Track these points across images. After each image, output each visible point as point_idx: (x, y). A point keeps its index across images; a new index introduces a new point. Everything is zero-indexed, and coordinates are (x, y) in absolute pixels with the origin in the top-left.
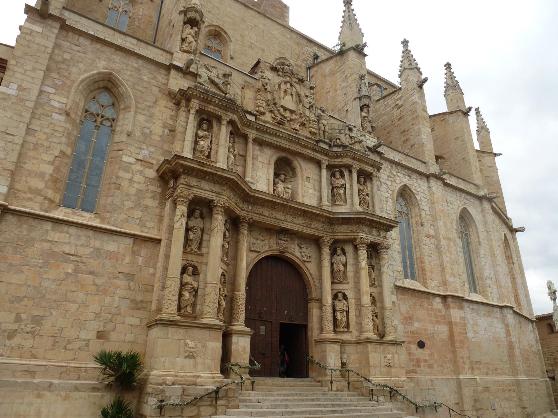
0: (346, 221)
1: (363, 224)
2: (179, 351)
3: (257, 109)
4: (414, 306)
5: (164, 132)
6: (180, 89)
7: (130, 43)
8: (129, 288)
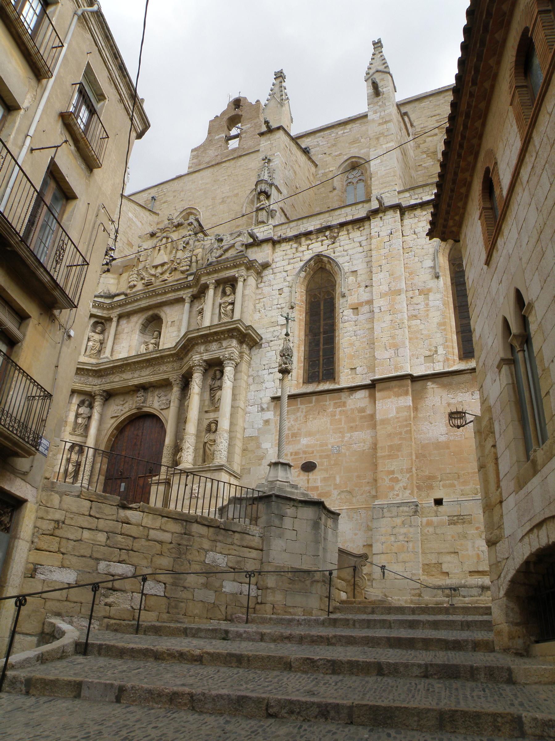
1: (197, 344)
6: (431, 234)
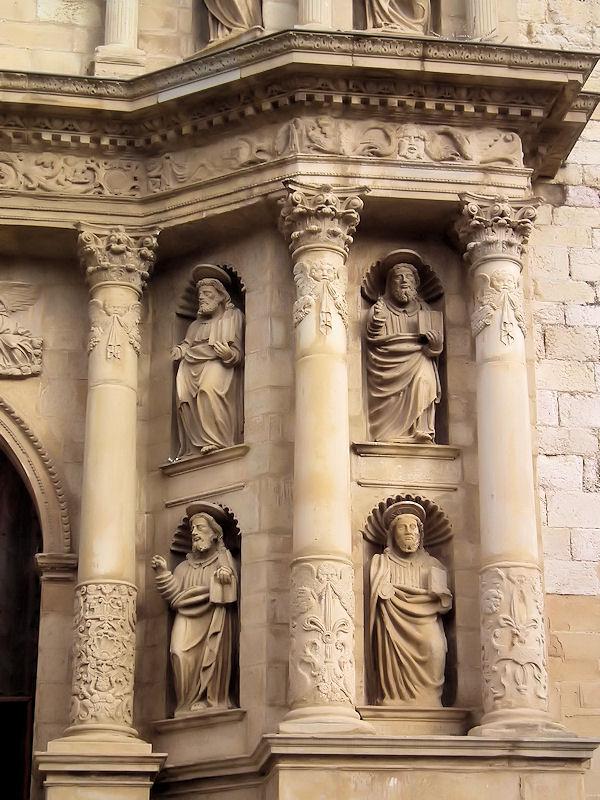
1: (315, 108)
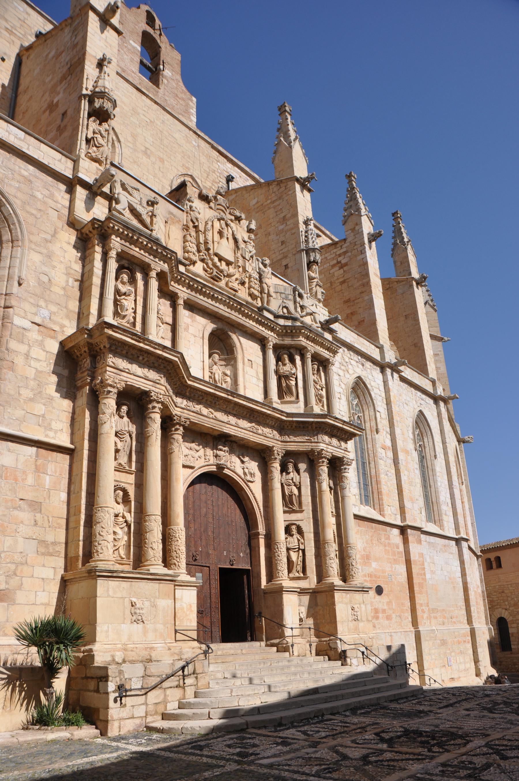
0: (301, 426)
2: (124, 614)
3: (186, 254)
4: (371, 540)
5: (67, 281)
7: (16, 137)
8: (36, 523)
